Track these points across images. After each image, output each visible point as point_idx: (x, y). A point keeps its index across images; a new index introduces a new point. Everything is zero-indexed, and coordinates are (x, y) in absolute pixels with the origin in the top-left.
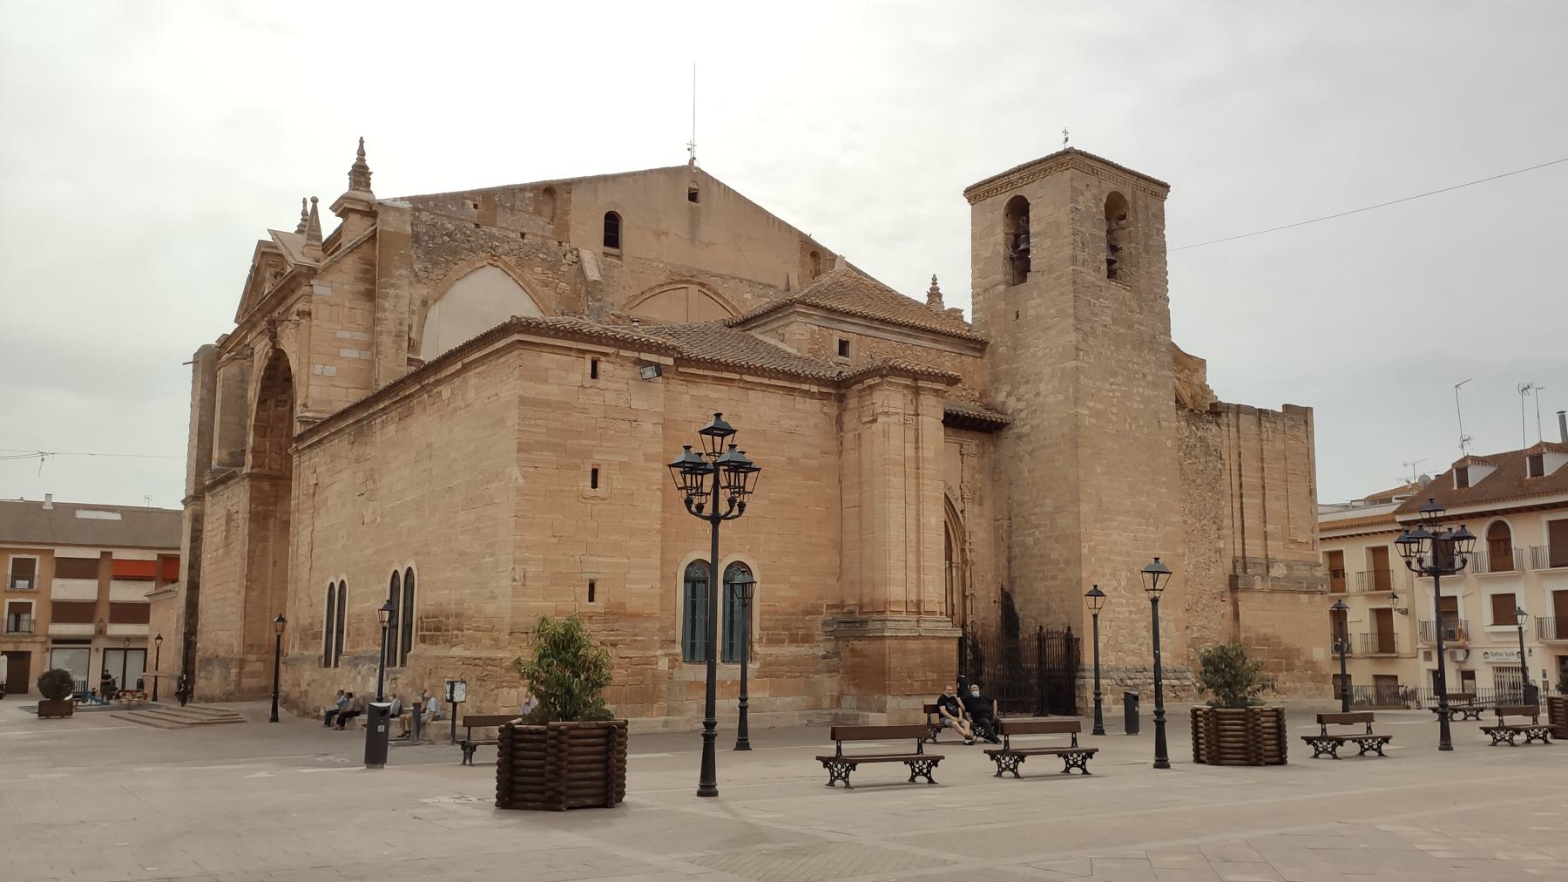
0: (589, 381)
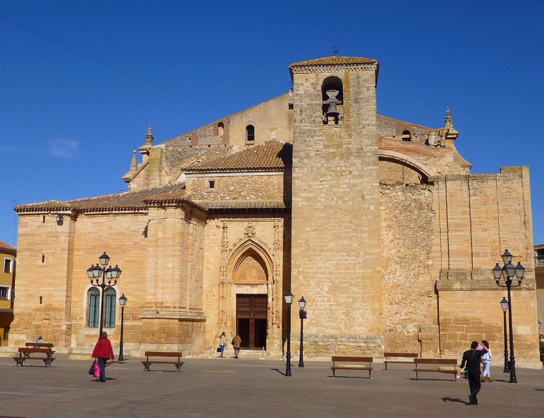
0: (42, 224)
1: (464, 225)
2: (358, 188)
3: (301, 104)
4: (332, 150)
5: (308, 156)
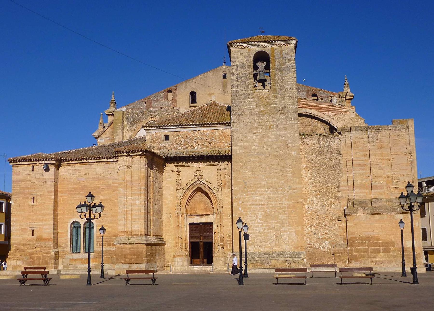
1: (365, 165)
2: (283, 138)
4: (262, 109)
5: (243, 114)
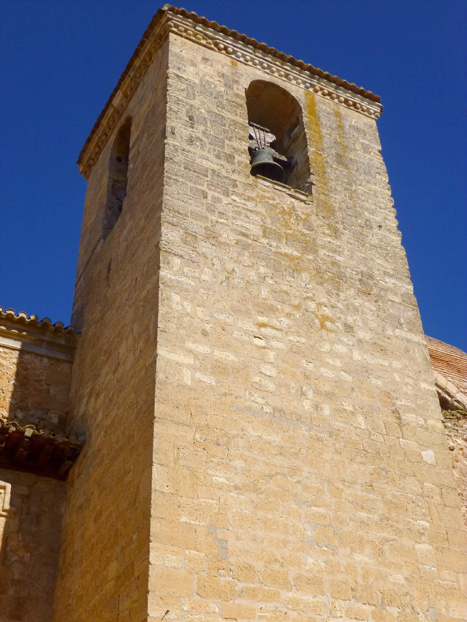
2: (380, 383)
3: (192, 102)
